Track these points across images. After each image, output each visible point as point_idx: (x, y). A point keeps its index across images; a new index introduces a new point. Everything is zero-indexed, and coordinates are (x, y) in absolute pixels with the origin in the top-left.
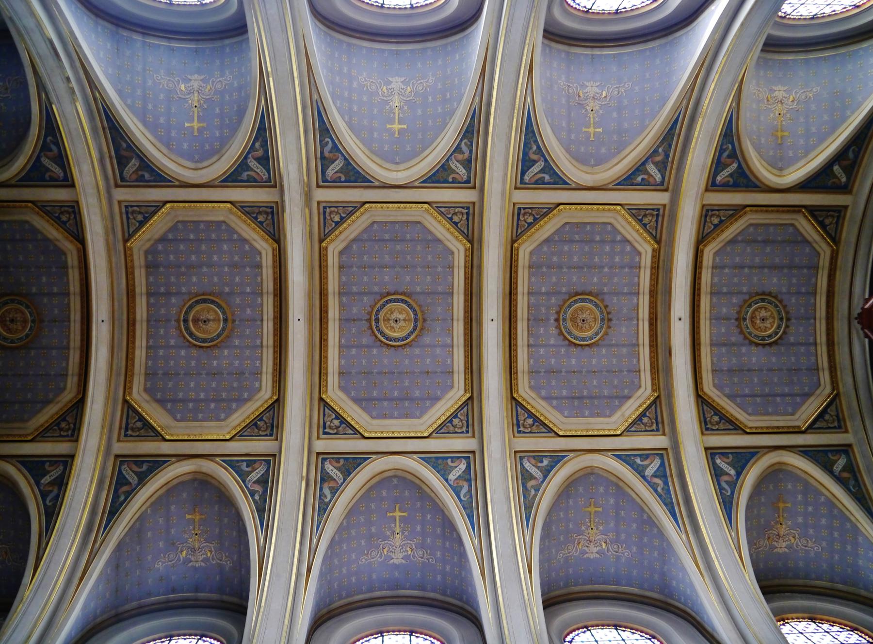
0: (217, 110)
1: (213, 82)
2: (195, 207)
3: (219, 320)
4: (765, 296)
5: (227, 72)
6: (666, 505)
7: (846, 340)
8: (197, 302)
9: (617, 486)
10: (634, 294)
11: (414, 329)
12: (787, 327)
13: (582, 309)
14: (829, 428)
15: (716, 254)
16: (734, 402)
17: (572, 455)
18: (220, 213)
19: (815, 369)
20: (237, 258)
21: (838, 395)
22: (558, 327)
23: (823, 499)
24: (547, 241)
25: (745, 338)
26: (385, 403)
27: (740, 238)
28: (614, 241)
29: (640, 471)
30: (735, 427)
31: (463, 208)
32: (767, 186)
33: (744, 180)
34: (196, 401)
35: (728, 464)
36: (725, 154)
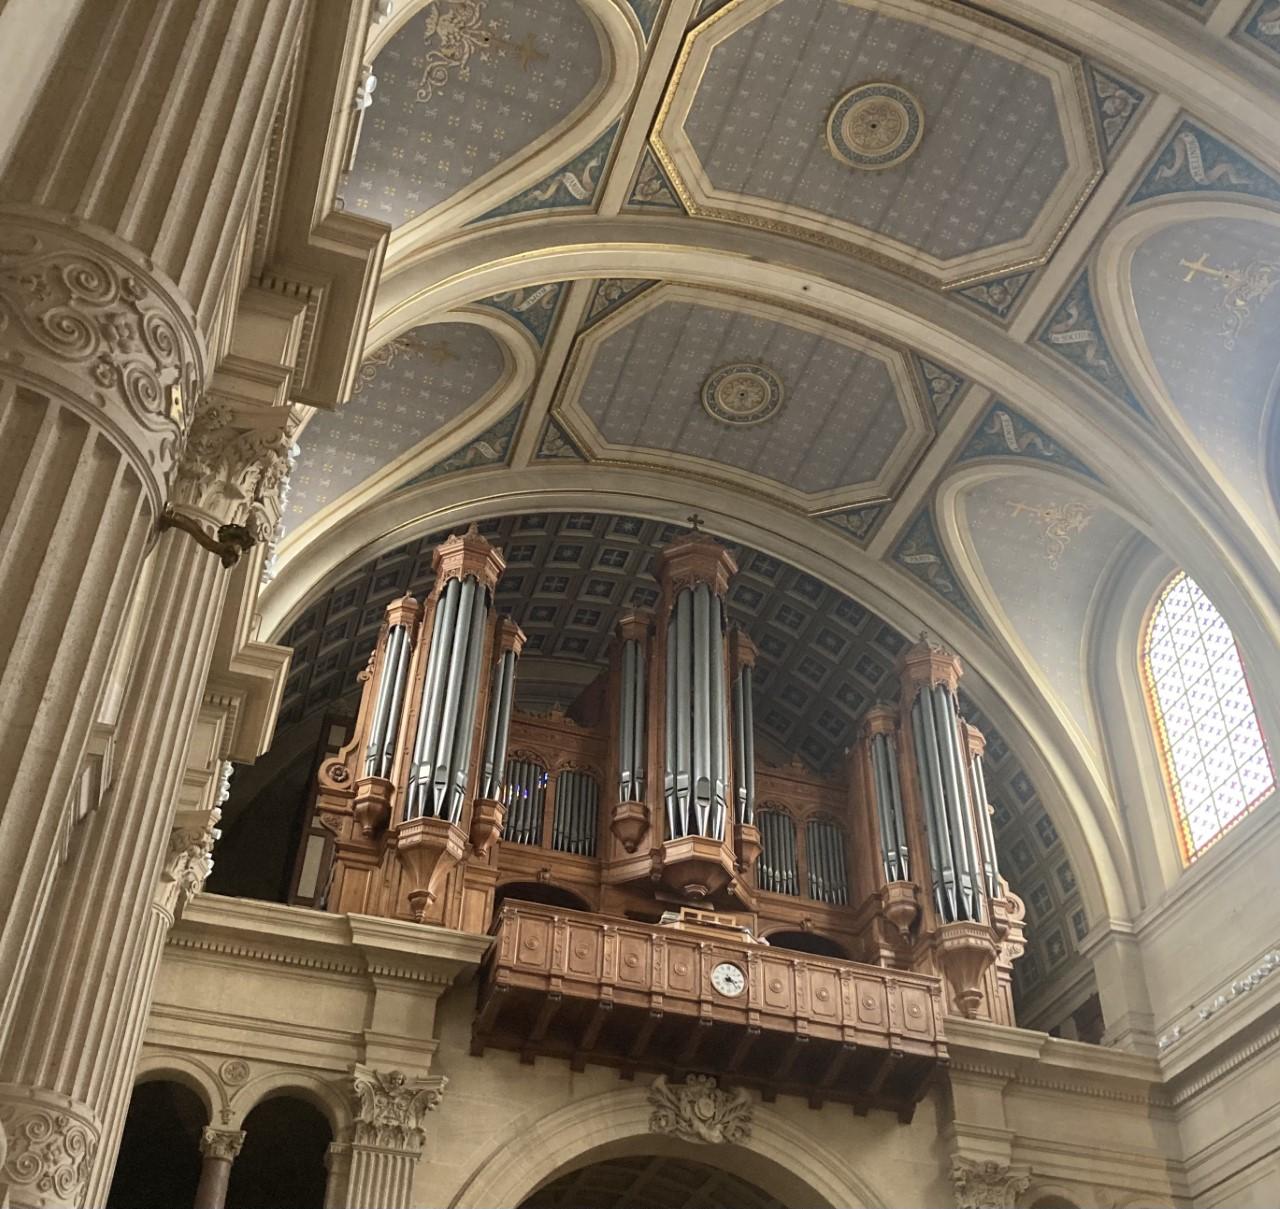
4: (777, 406)
6: (509, 202)
12: (717, 422)
15: (882, 366)
19: (637, 441)
21: (587, 461)
23: (440, 418)
27: (890, 406)
30: (590, 321)
32: (953, 472)
33: (981, 445)
35: (540, 301)
36: (1038, 441)
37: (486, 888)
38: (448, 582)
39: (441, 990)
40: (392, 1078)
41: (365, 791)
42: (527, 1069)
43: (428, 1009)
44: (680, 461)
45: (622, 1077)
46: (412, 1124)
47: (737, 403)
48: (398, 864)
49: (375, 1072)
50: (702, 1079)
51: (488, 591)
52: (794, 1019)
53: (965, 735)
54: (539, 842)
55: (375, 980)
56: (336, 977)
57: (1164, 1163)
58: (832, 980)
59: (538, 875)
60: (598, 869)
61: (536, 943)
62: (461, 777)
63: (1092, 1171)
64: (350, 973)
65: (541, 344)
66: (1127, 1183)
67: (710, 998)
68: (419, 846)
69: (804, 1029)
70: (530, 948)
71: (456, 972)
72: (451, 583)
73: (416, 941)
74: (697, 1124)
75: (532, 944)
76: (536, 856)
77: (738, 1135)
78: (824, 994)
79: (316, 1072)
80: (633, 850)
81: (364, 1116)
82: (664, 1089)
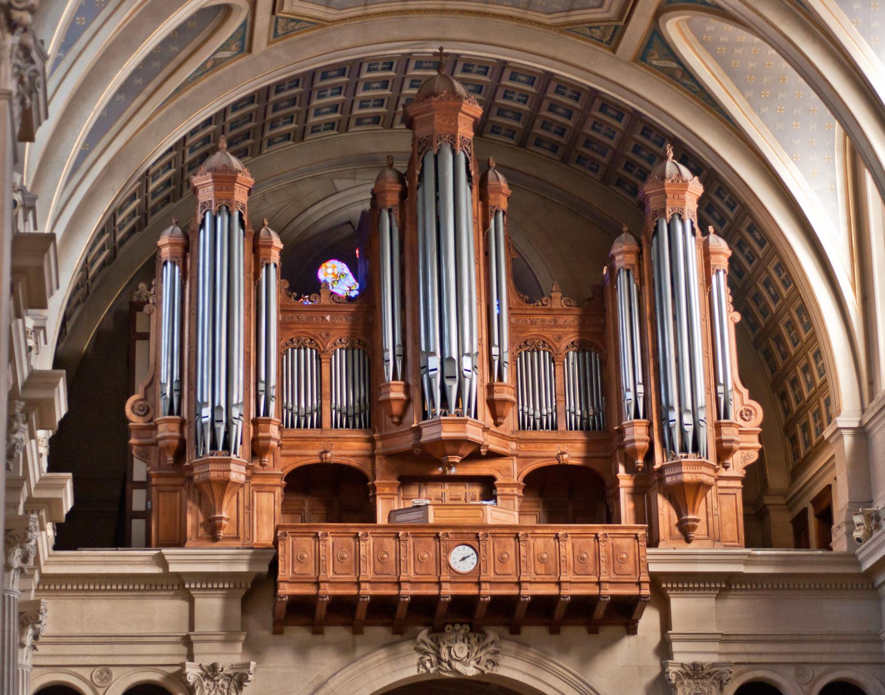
21: (323, 26)
37: (272, 489)
38: (205, 214)
39: (243, 592)
40: (214, 667)
45: (395, 633)
48: (196, 491)
49: (200, 665)
50: (457, 627)
51: (241, 215)
53: (706, 254)
54: (320, 425)
55: (192, 592)
56: (162, 593)
61: (306, 556)
62: (235, 412)
63: (793, 654)
64: (173, 589)
66: (825, 659)
67: (448, 578)
70: (301, 560)
71: (253, 578)
72: (208, 214)
73: (217, 562)
74: (453, 663)
75: (302, 558)
76: (317, 439)
77: (490, 666)
78: (545, 556)
79: (160, 668)
80: (399, 424)
82: (428, 640)
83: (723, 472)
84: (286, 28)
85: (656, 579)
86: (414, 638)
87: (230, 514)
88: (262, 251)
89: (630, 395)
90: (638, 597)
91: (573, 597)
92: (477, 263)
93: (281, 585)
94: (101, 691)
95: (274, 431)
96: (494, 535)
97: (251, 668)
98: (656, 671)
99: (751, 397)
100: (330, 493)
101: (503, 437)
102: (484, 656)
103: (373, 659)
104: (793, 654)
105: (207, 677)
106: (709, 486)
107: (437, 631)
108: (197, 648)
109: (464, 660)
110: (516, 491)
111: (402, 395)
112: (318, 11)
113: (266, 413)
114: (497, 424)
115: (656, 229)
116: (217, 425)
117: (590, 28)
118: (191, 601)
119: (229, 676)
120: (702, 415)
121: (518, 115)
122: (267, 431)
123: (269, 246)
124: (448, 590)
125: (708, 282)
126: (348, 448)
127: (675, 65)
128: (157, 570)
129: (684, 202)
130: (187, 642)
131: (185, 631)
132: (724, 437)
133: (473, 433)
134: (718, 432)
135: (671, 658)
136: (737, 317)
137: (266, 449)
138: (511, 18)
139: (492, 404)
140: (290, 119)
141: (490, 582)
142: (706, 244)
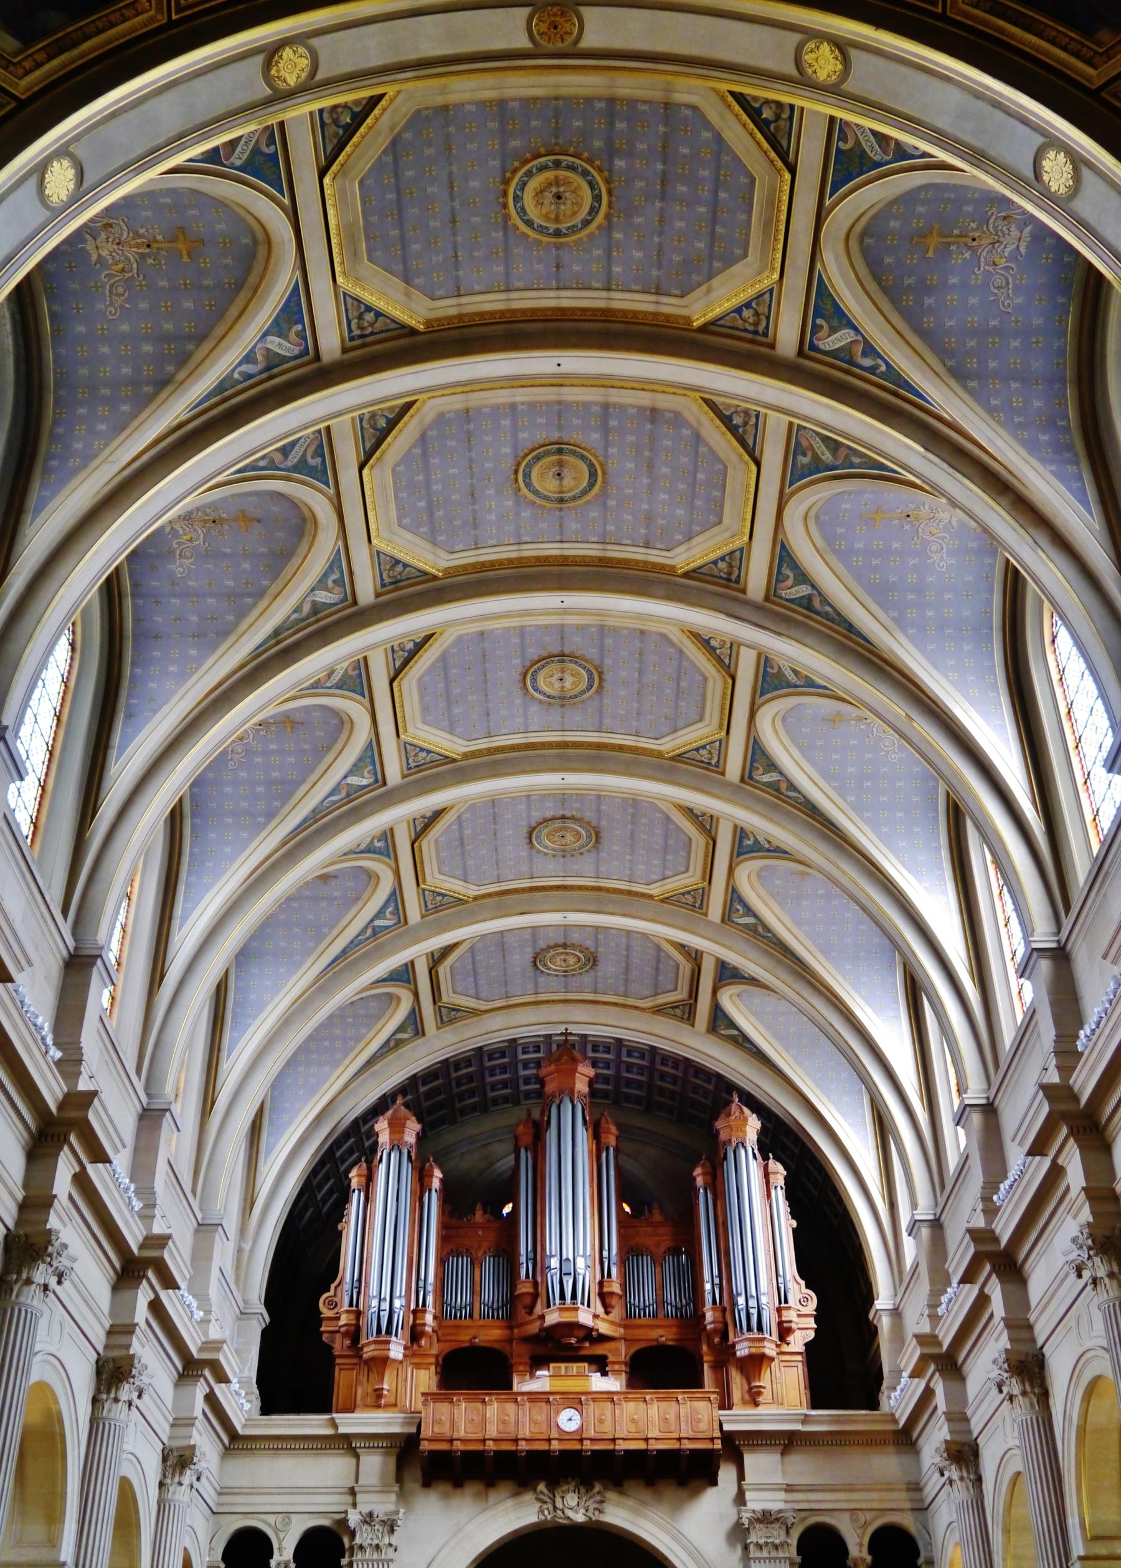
0: (896, 545)
1: (943, 538)
2: (746, 505)
3: (561, 492)
4: (593, 961)
5: (953, 561)
7: (543, 1020)
8: (591, 466)
9: (357, 899)
10: (598, 871)
11: (549, 697)
13: (579, 834)
14: (441, 1017)
16: (466, 952)
17: (393, 864)
18: (734, 511)
20: (660, 521)
21: (478, 1015)
22: (554, 819)
23: (364, 1031)
24: (681, 652)
25: (542, 950)
26: (391, 196)
27: (662, 954)
28: (664, 868)
29: (380, 914)
31: (718, 761)
32: (721, 987)
34: (428, 483)
39: (396, 1450)
40: (371, 1514)
41: (344, 1319)
42: (459, 1490)
43: (392, 1461)
44: (542, 997)
46: (386, 1540)
47: (563, 964)
50: (570, 1480)
51: (409, 1152)
52: (614, 1440)
53: (767, 1175)
54: (471, 1316)
57: (904, 1486)
58: (642, 1405)
59: (470, 1341)
60: (511, 1328)
62: (397, 1303)
63: (848, 1501)
65: (409, 983)
66: (875, 1505)
67: (556, 1436)
68: (373, 1359)
69: (622, 1446)
70: (440, 1422)
73: (376, 1424)
76: (468, 1327)
77: (597, 1513)
80: (530, 1313)
81: (358, 1540)
83: (785, 1348)
84: (448, 1016)
85: (728, 1438)
86: (535, 1490)
87: (390, 1385)
88: (426, 1179)
89: (708, 1286)
90: (712, 1451)
91: (658, 1451)
92: (592, 1186)
93: (422, 1443)
94: (282, 1535)
95: (429, 1318)
96: (594, 1400)
97: (401, 1515)
98: (734, 1518)
99: (807, 1287)
100: (473, 1370)
101: (612, 1323)
102: (592, 1505)
103: (501, 1507)
104: (848, 1501)
105: (365, 1522)
106: (772, 1359)
107: (553, 1486)
108: (359, 1497)
109: (574, 1508)
110: (623, 1368)
111: (531, 1290)
112: (471, 1003)
113: (424, 1304)
114: (607, 1313)
115: (725, 1154)
116: (382, 1313)
117: (673, 1008)
118: (357, 1457)
119: (383, 1521)
120: (764, 1300)
121: (639, 1085)
122: (424, 1318)
123: (432, 1176)
124: (555, 1446)
125: (769, 1195)
126: (491, 1334)
127: (736, 1032)
128: (329, 1431)
129: (745, 1132)
130: (352, 1492)
131: (351, 1484)
132: (784, 1319)
133: (584, 1317)
134: (780, 1316)
135: (745, 1505)
136: (794, 1224)
137: (423, 1334)
138: (616, 1004)
139: (603, 1296)
140: (472, 1093)
141: (591, 1439)
142: (766, 1168)
